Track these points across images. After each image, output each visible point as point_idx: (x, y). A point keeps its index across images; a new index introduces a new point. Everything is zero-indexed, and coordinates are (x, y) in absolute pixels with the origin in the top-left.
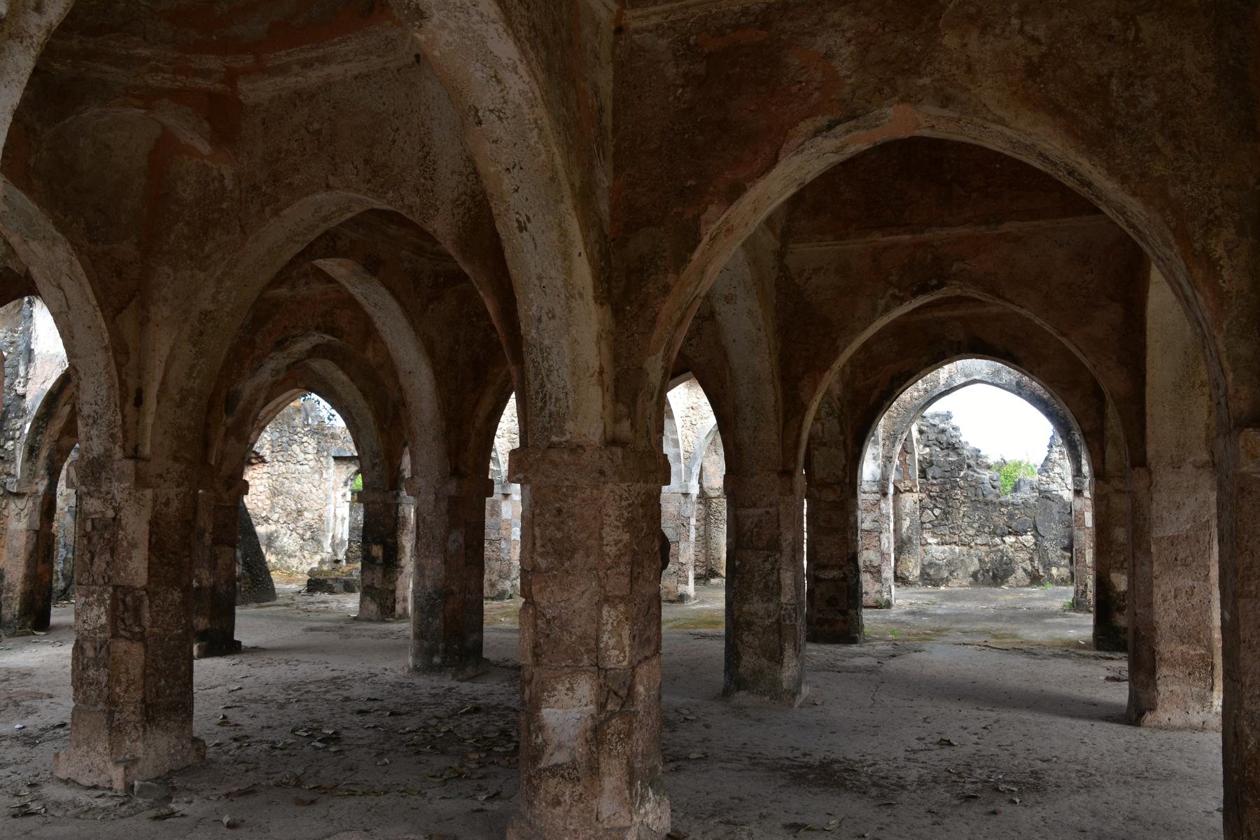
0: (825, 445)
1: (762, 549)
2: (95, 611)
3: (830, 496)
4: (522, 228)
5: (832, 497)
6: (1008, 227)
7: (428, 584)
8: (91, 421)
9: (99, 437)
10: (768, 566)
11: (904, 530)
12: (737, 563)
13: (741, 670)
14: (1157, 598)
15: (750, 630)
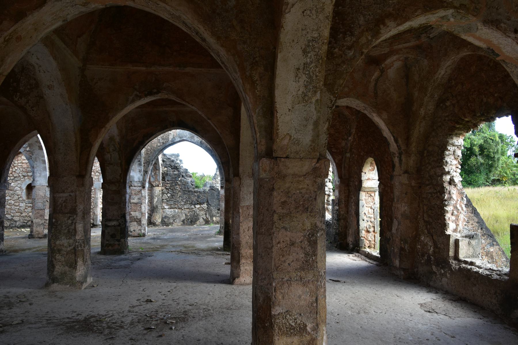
0: (112, 164)
1: (67, 213)
5: (114, 188)
6: (188, 69)
10: (70, 222)
11: (155, 203)
12: (54, 220)
13: (55, 273)
14: (241, 231)
15: (60, 253)
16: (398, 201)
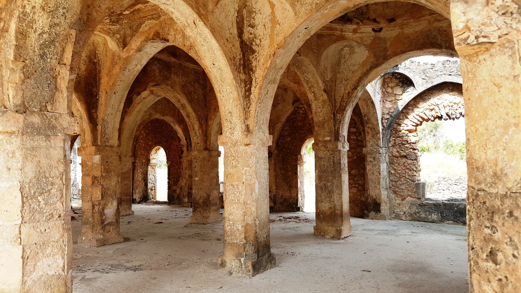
4: (115, 93)
16: (186, 169)
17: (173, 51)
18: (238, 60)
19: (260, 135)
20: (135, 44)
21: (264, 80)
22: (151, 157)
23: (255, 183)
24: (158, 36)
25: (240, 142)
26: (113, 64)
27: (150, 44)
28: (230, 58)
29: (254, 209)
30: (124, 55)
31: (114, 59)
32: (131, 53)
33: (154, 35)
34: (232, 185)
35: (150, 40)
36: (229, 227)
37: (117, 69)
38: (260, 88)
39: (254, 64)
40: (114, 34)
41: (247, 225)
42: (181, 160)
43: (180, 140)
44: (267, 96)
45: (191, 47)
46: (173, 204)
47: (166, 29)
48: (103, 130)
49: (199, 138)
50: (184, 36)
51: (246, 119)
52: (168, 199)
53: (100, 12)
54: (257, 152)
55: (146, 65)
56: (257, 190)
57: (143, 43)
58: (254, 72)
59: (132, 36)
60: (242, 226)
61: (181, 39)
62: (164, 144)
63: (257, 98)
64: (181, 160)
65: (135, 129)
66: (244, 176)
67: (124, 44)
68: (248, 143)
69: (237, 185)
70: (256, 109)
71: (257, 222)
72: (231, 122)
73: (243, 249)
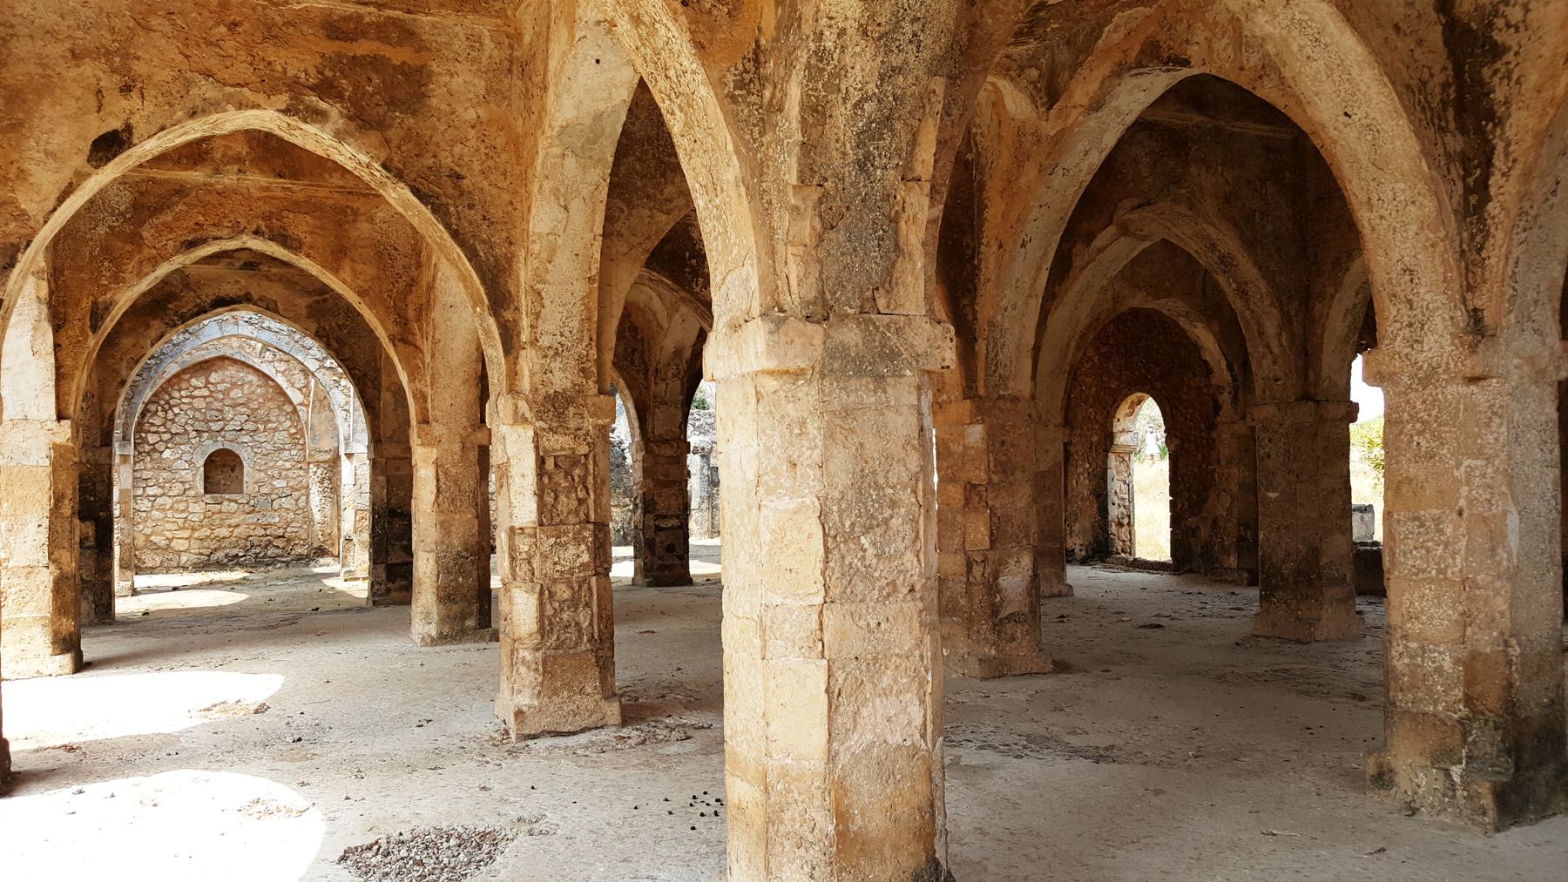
2: (572, 550)
3: (668, 451)
4: (1023, 245)
5: (669, 452)
7: (456, 542)
8: (551, 353)
9: (564, 371)
16: (1229, 463)
17: (1199, 93)
18: (1438, 90)
19: (1528, 342)
20: (1081, 91)
21: (1542, 144)
22: (1117, 427)
23: (1505, 513)
24: (1153, 54)
25: (1447, 370)
26: (1020, 158)
27: (1128, 82)
28: (1408, 87)
29: (1501, 604)
30: (1050, 128)
31: (1021, 143)
32: (1071, 120)
33: (1142, 51)
34: (1416, 519)
35: (1130, 69)
36: (1406, 661)
37: (1031, 171)
38: (1526, 176)
39: (1499, 95)
40: (1022, 68)
41: (1474, 656)
42: (1214, 435)
43: (1207, 370)
44: (1553, 200)
45: (1269, 68)
46: (1190, 571)
47: (1182, 27)
48: (992, 355)
49: (1280, 361)
50: (1240, 41)
51: (1470, 288)
52: (1173, 554)
53: (1002, 12)
54: (1514, 405)
55: (1117, 147)
56: (1513, 541)
57: (1107, 83)
58: (1500, 123)
59: (1075, 66)
60: (1457, 662)
61: (1230, 51)
62: (1158, 385)
63: (1514, 211)
64: (1214, 435)
65: (1073, 345)
66: (1465, 490)
67: (1050, 93)
68: (1478, 371)
69: (1438, 521)
70: (1509, 252)
71: (1515, 651)
72: (1410, 302)
73: (1458, 736)
